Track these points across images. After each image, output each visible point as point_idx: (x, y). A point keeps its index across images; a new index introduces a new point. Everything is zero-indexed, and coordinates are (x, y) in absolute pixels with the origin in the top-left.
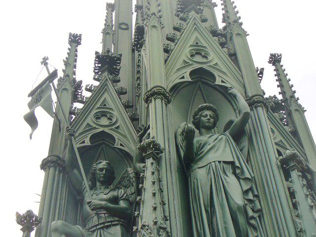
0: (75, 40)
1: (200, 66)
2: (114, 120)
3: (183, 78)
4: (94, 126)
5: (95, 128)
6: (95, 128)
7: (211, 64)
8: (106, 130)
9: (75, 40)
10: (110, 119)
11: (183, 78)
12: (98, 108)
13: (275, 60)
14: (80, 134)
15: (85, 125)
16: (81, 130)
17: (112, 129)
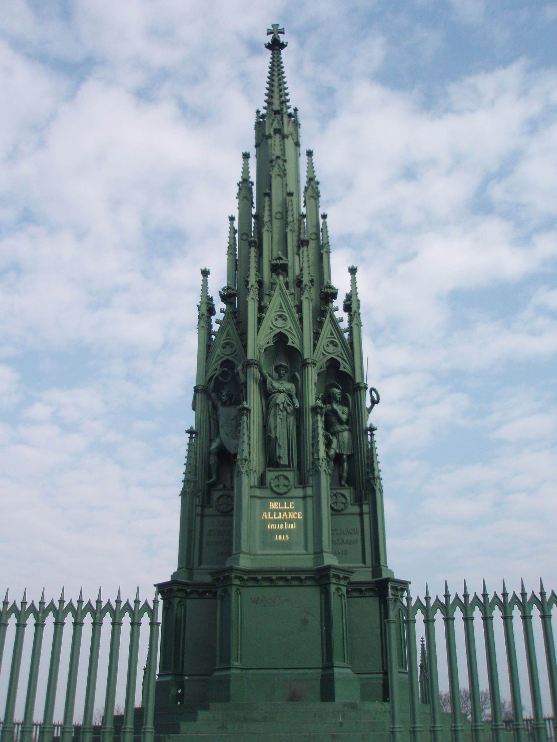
0: (205, 273)
1: (278, 331)
2: (234, 349)
3: (268, 343)
4: (222, 355)
5: (222, 357)
6: (222, 357)
7: (286, 328)
8: (230, 358)
9: (205, 273)
10: (232, 347)
11: (268, 343)
12: (224, 340)
13: (353, 271)
14: (215, 363)
15: (216, 355)
16: (214, 361)
17: (233, 357)
